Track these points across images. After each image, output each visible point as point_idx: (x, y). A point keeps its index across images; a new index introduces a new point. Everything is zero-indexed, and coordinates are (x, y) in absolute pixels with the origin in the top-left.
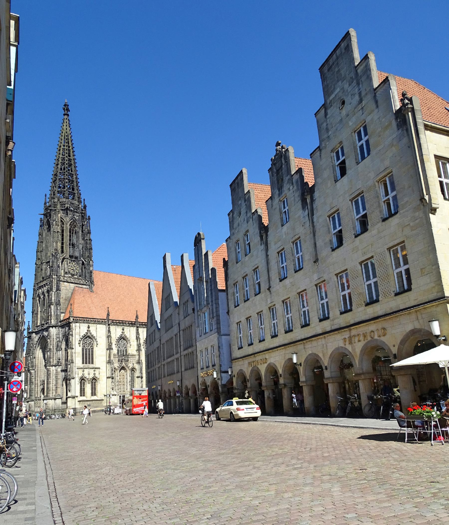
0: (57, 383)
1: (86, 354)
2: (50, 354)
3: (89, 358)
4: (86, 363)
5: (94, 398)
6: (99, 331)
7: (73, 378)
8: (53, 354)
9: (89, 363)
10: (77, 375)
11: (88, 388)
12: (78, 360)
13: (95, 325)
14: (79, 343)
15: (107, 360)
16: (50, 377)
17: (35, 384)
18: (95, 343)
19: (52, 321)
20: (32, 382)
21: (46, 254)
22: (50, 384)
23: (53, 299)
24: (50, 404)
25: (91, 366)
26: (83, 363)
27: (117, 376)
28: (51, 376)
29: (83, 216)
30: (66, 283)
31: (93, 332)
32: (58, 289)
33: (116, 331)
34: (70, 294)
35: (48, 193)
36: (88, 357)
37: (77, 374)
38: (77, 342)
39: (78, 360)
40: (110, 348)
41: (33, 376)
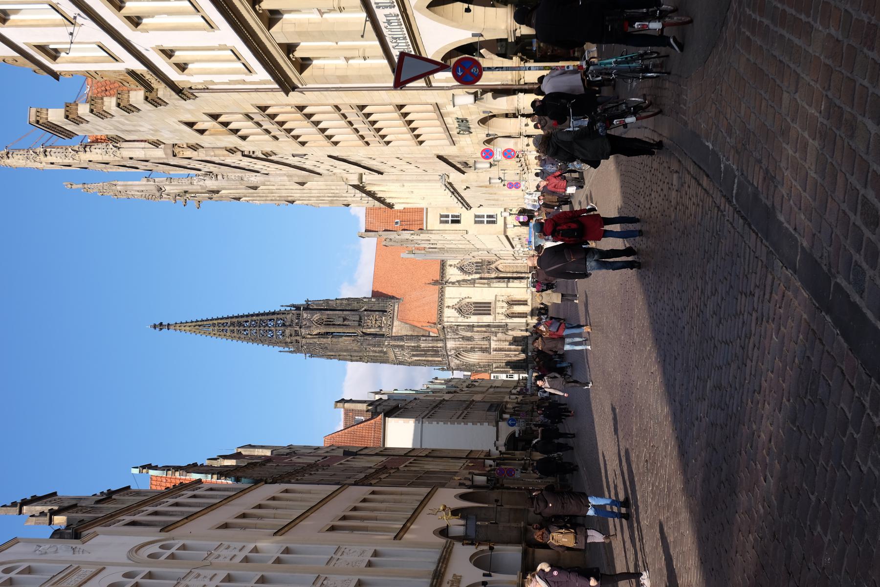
5: (529, 303)
6: (453, 295)
11: (518, 309)
12: (487, 319)
13: (446, 300)
18: (468, 300)
19: (439, 345)
21: (355, 351)
25: (492, 305)
26: (490, 314)
29: (307, 308)
30: (394, 330)
31: (455, 301)
32: (401, 338)
33: (453, 274)
35: (277, 349)
36: (483, 308)
37: (501, 319)
38: (466, 320)
39: (487, 319)
40: (473, 282)
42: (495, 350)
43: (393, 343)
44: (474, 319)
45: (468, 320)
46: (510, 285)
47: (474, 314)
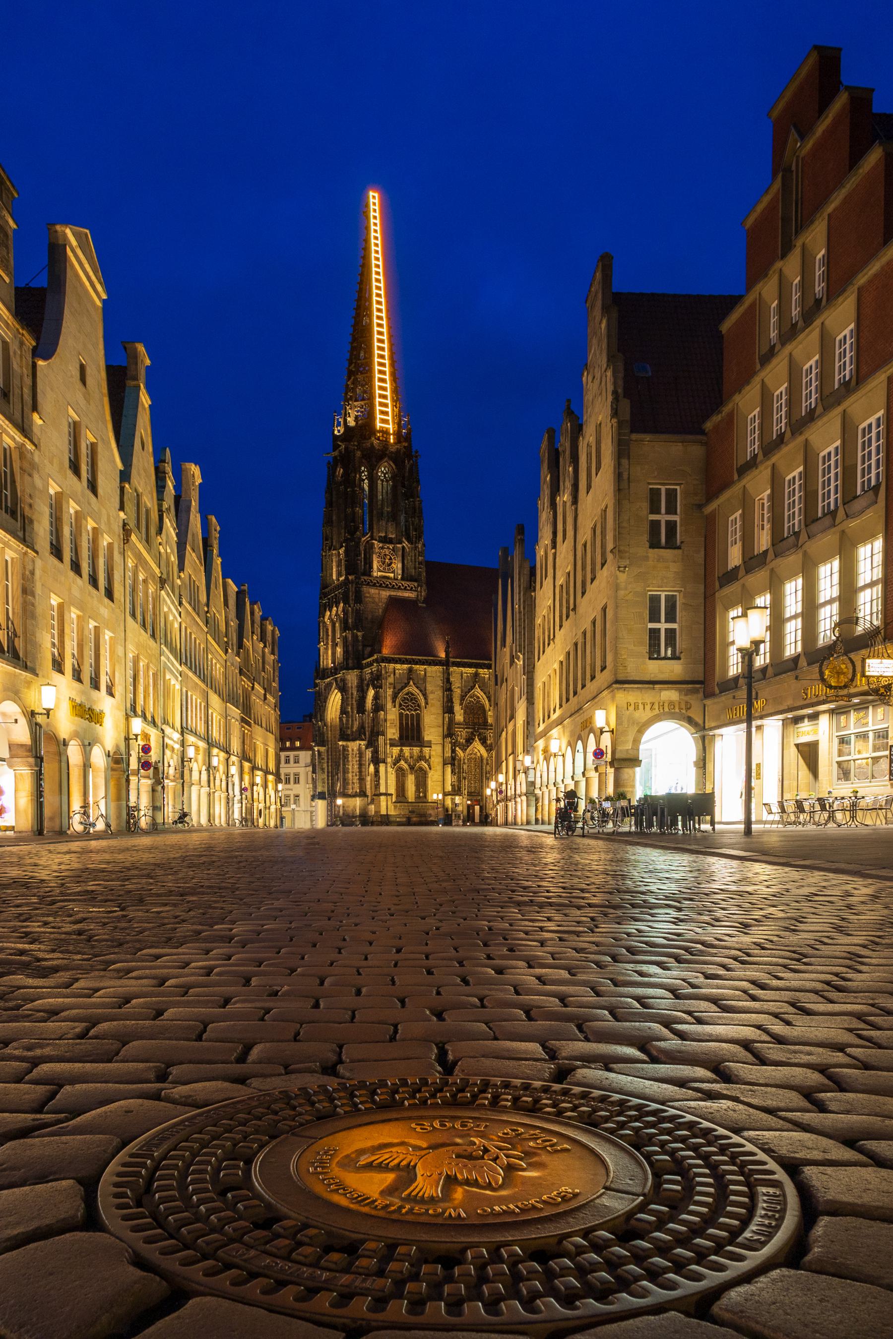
0: (360, 772)
1: (407, 724)
2: (347, 721)
3: (412, 730)
4: (407, 738)
7: (384, 761)
8: (352, 721)
9: (413, 738)
10: (389, 760)
12: (393, 732)
14: (394, 702)
15: (446, 733)
16: (348, 761)
17: (328, 772)
19: (350, 661)
20: (323, 769)
22: (348, 772)
23: (350, 621)
24: (348, 807)
26: (401, 737)
27: (464, 763)
28: (350, 759)
30: (373, 591)
34: (380, 611)
41: (323, 759)
42: (345, 748)
43: (352, 588)
44: (392, 715)
45: (389, 705)
46: (449, 769)
47: (401, 715)
